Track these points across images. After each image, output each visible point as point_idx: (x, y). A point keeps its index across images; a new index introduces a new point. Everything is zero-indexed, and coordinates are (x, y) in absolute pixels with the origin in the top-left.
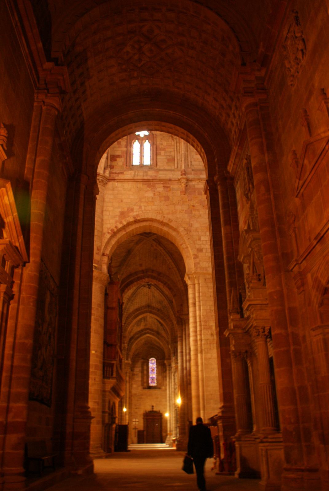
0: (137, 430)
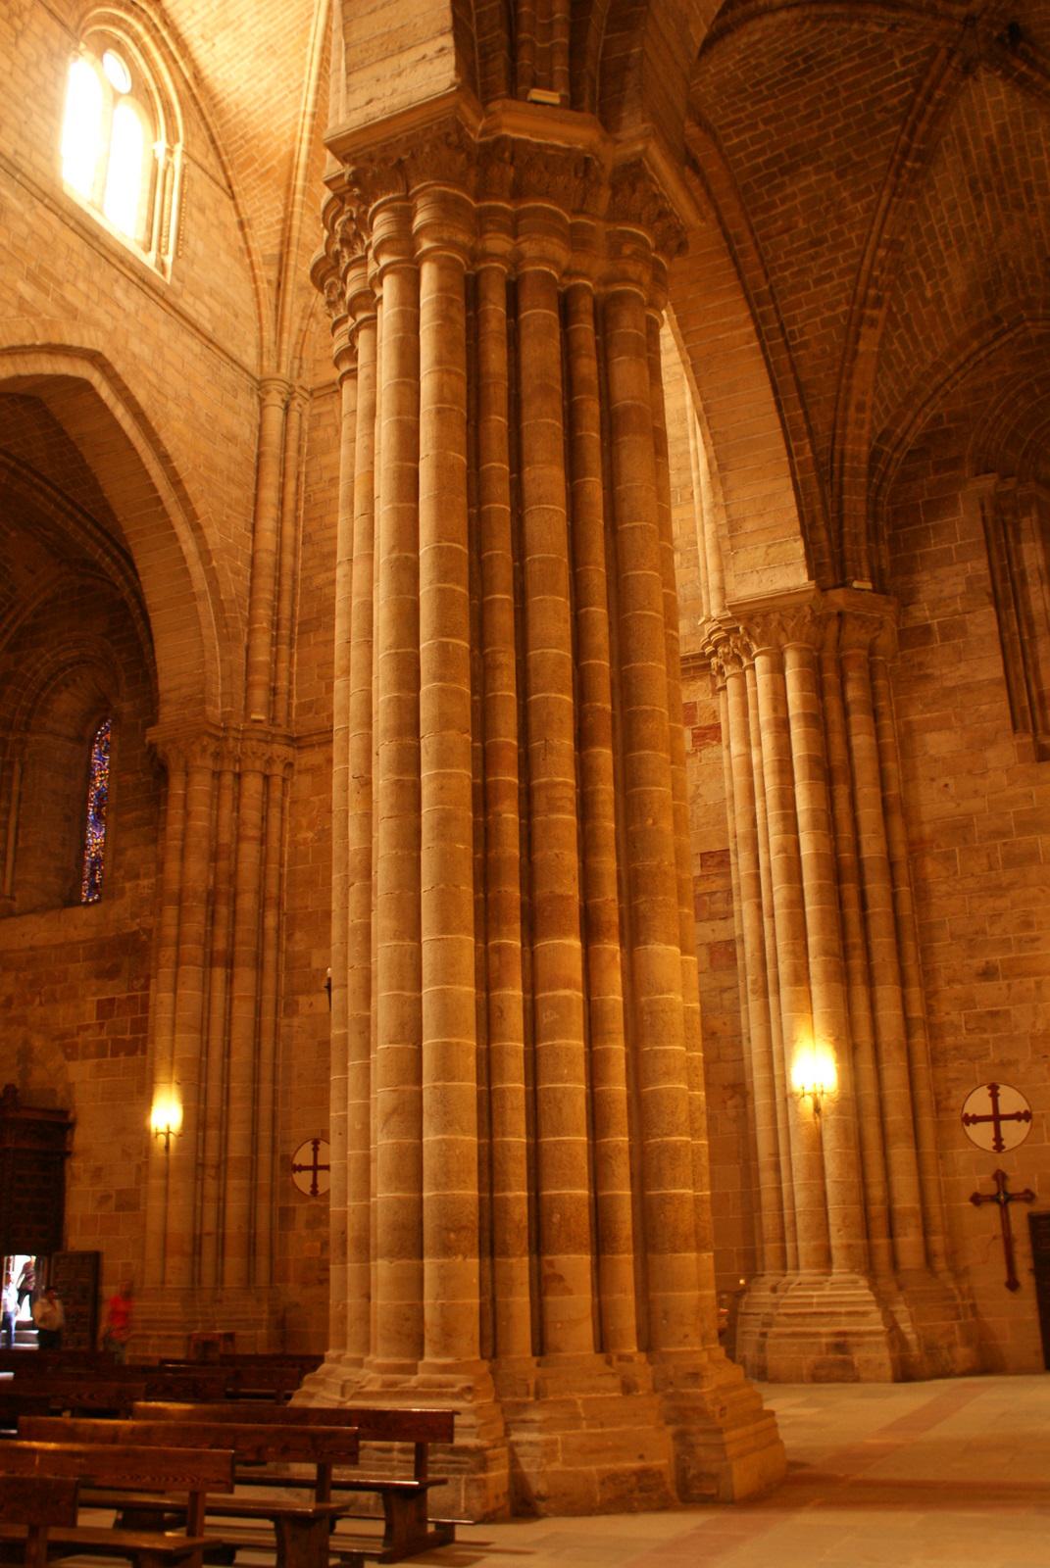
0: (1019, 1213)
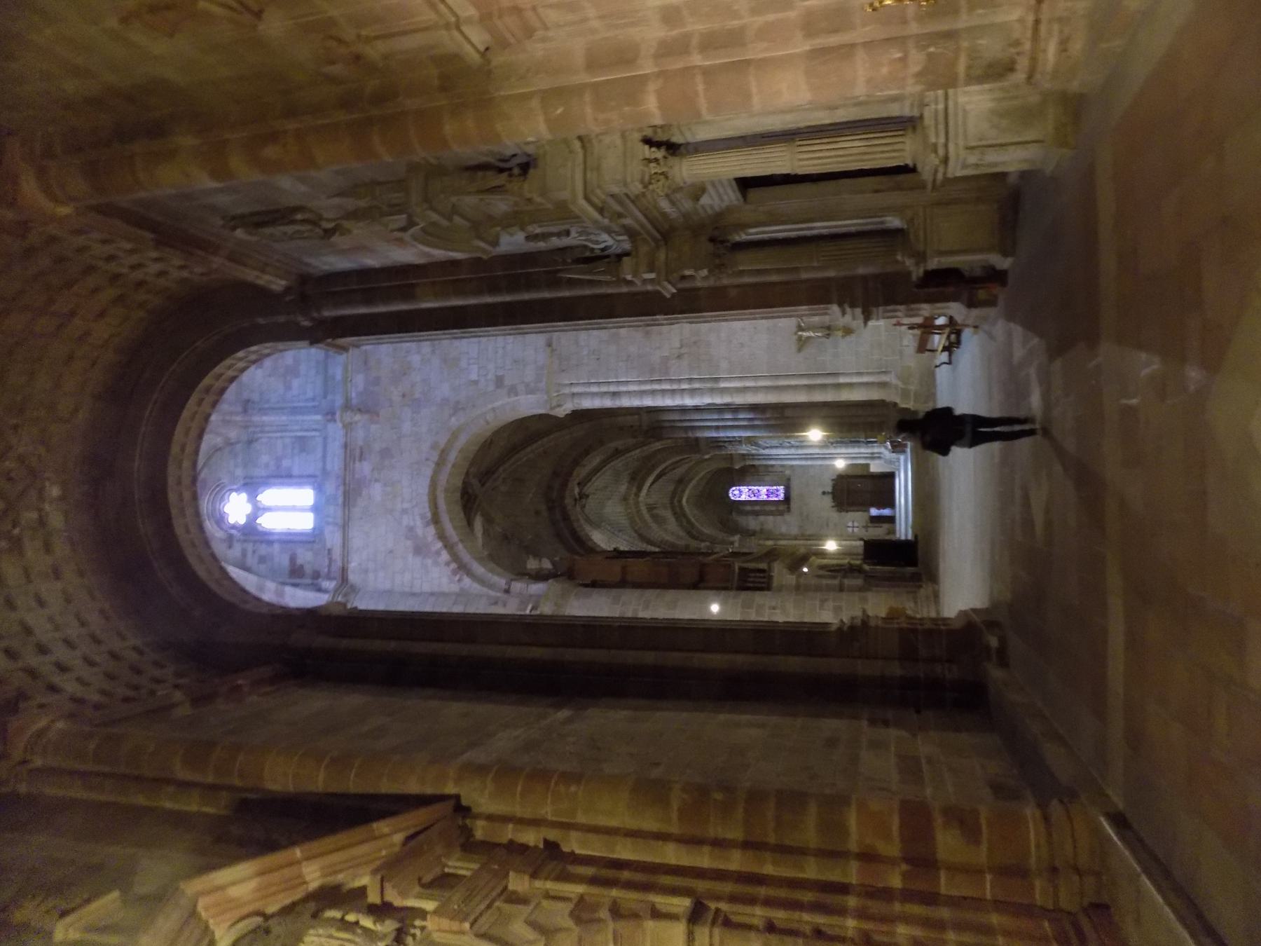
0: (869, 525)
